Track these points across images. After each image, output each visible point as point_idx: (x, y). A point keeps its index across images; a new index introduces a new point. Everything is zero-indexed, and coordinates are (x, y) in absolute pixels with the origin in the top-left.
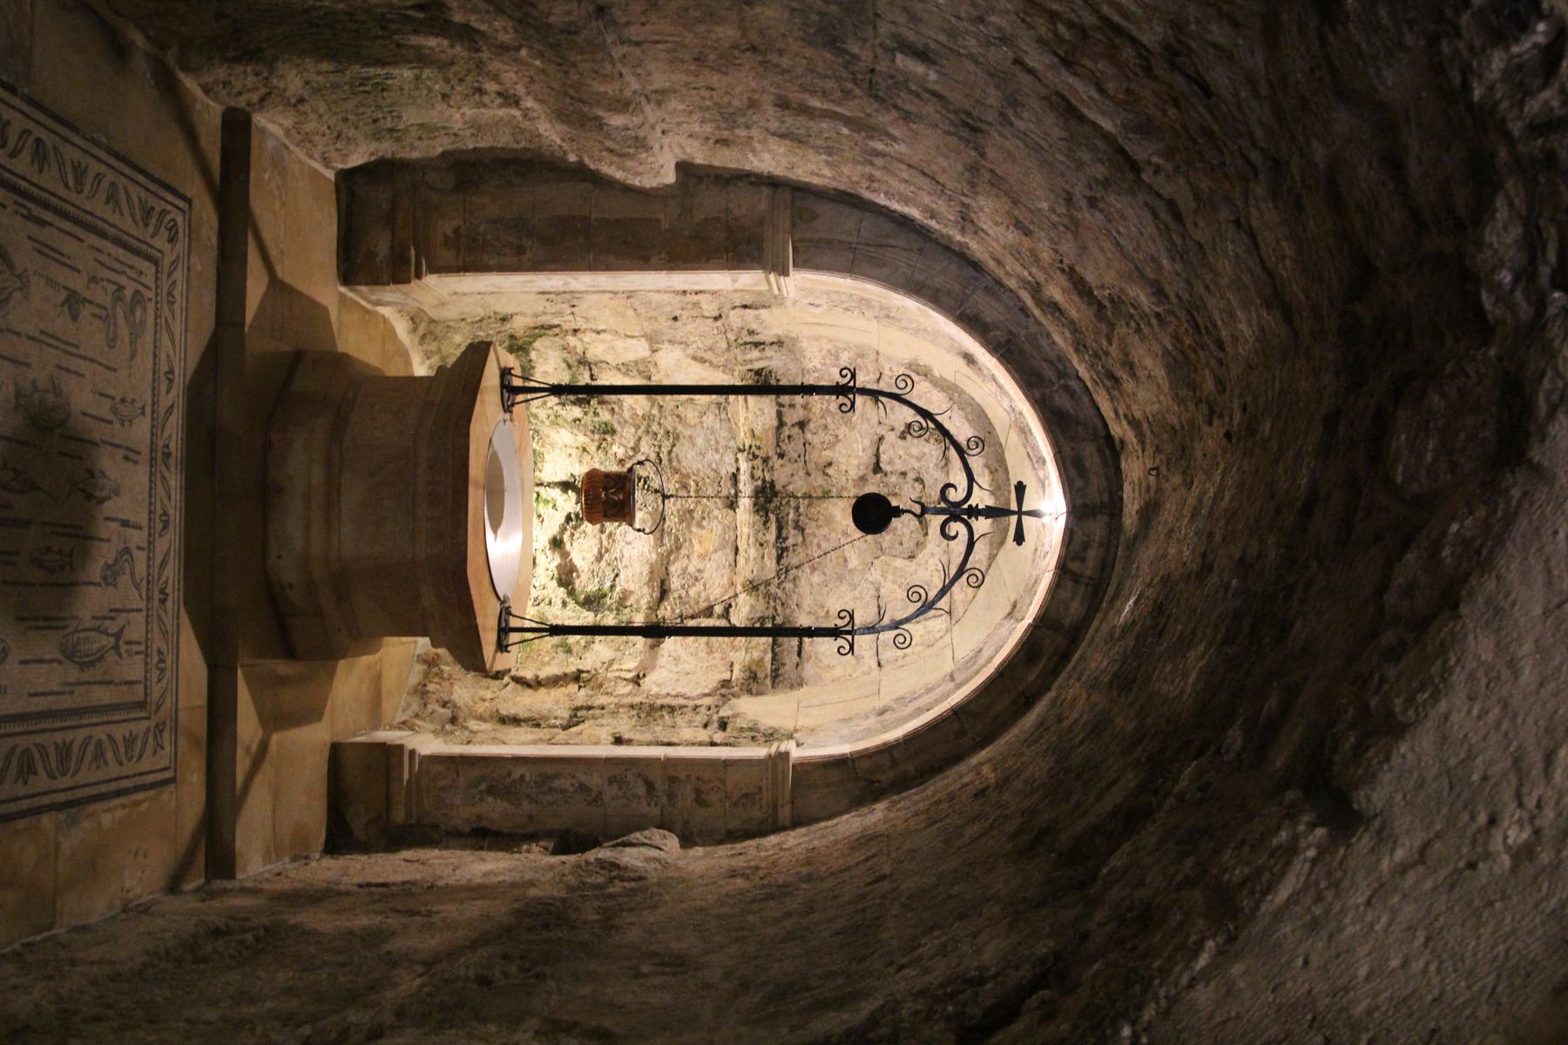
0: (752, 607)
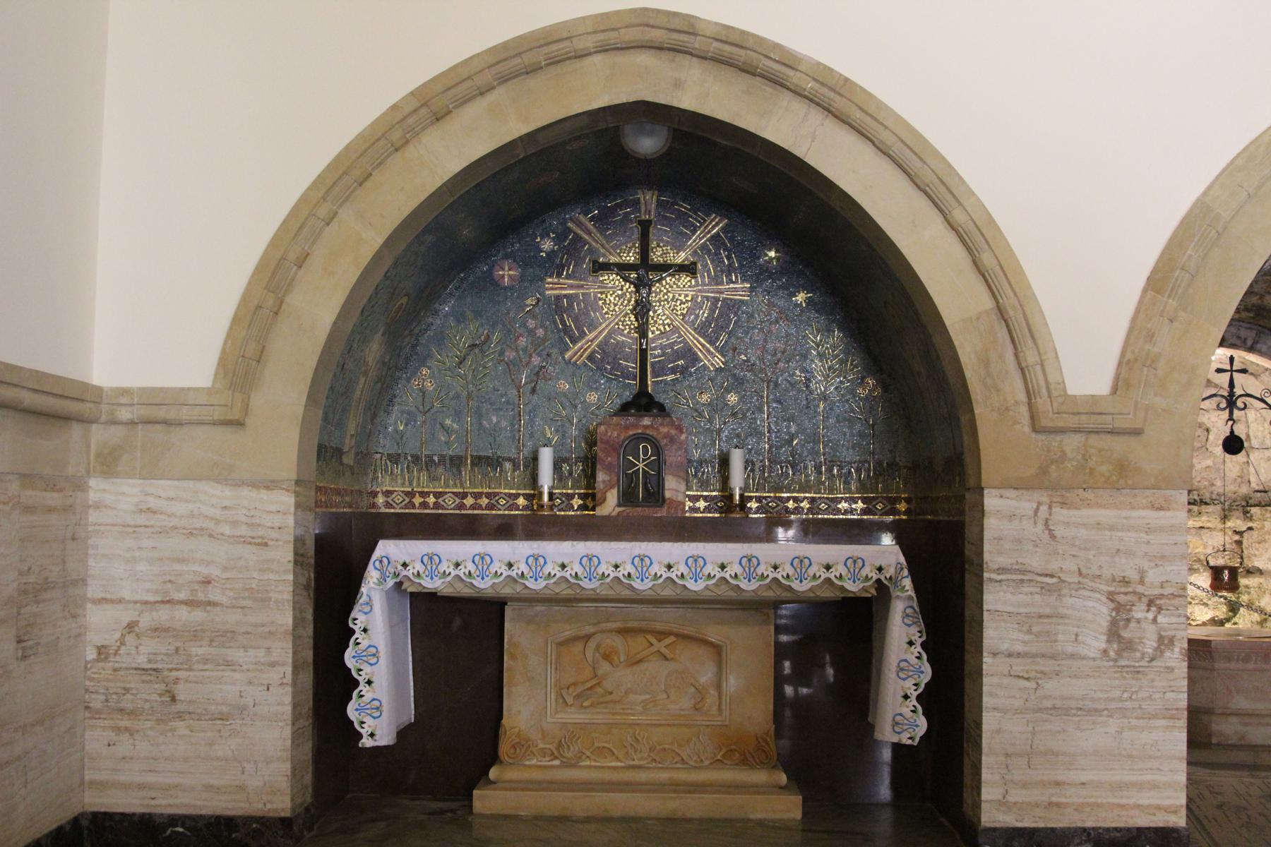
0: (1237, 518)
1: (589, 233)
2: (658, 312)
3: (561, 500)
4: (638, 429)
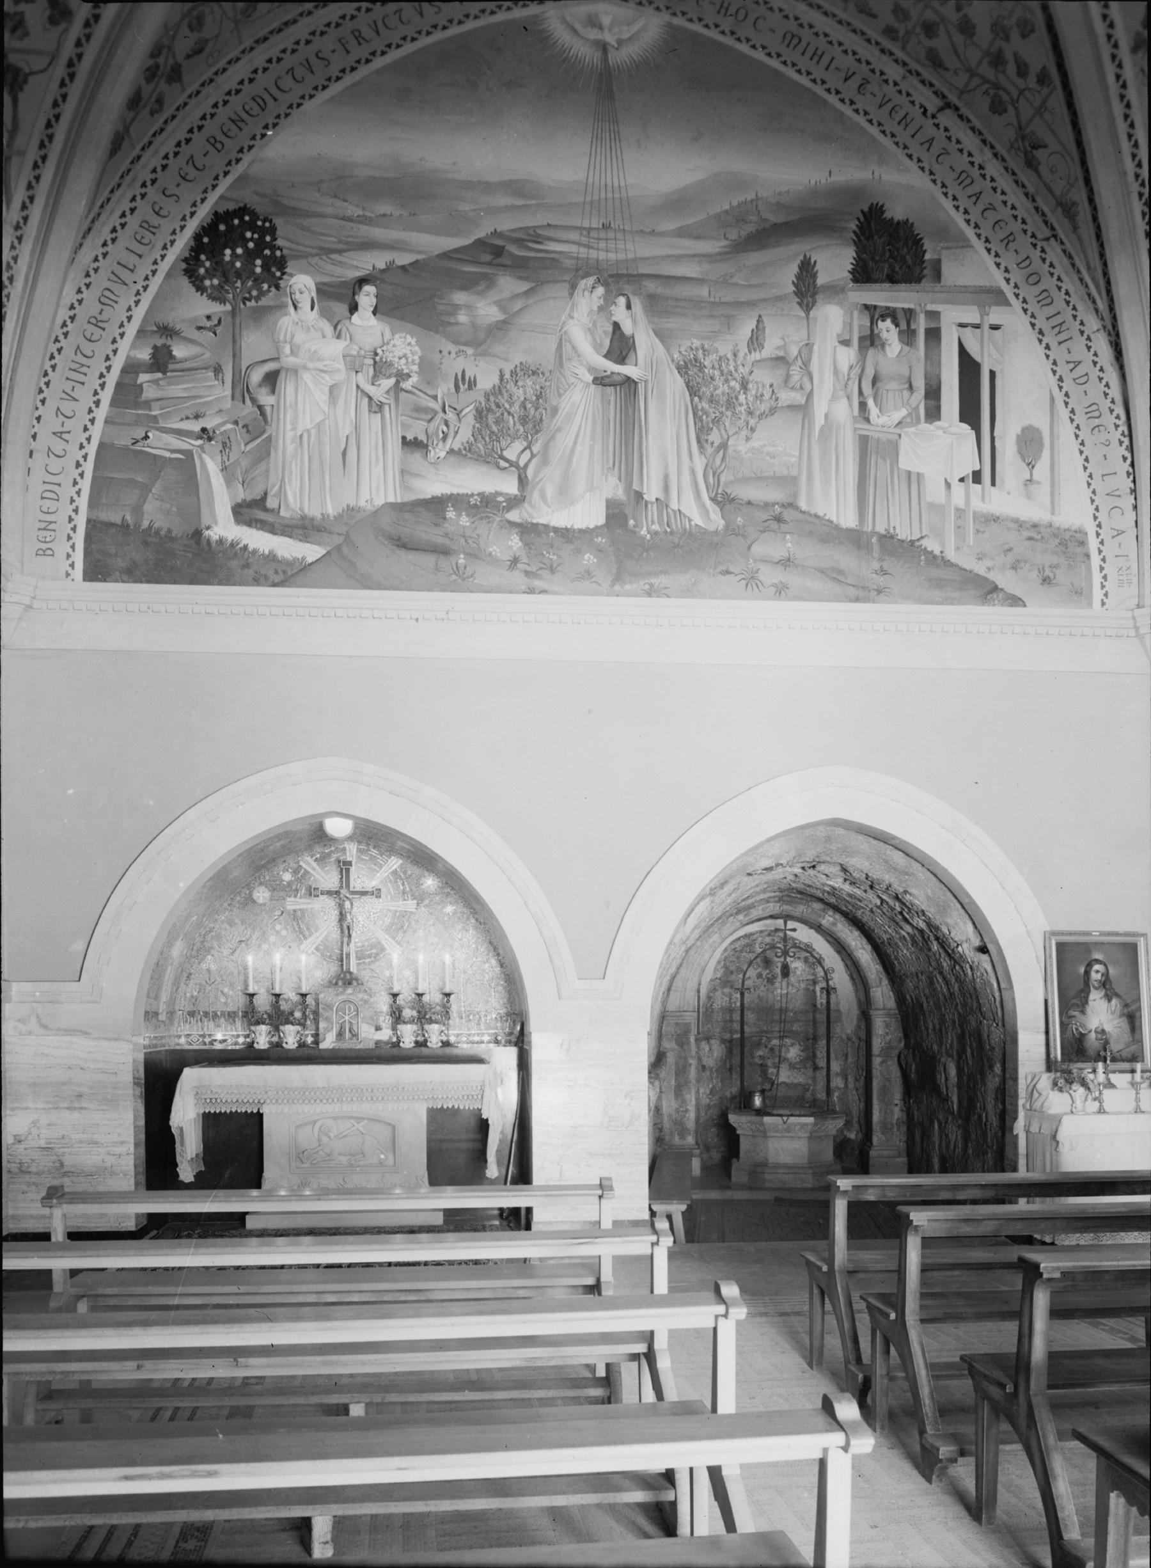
1: (314, 869)
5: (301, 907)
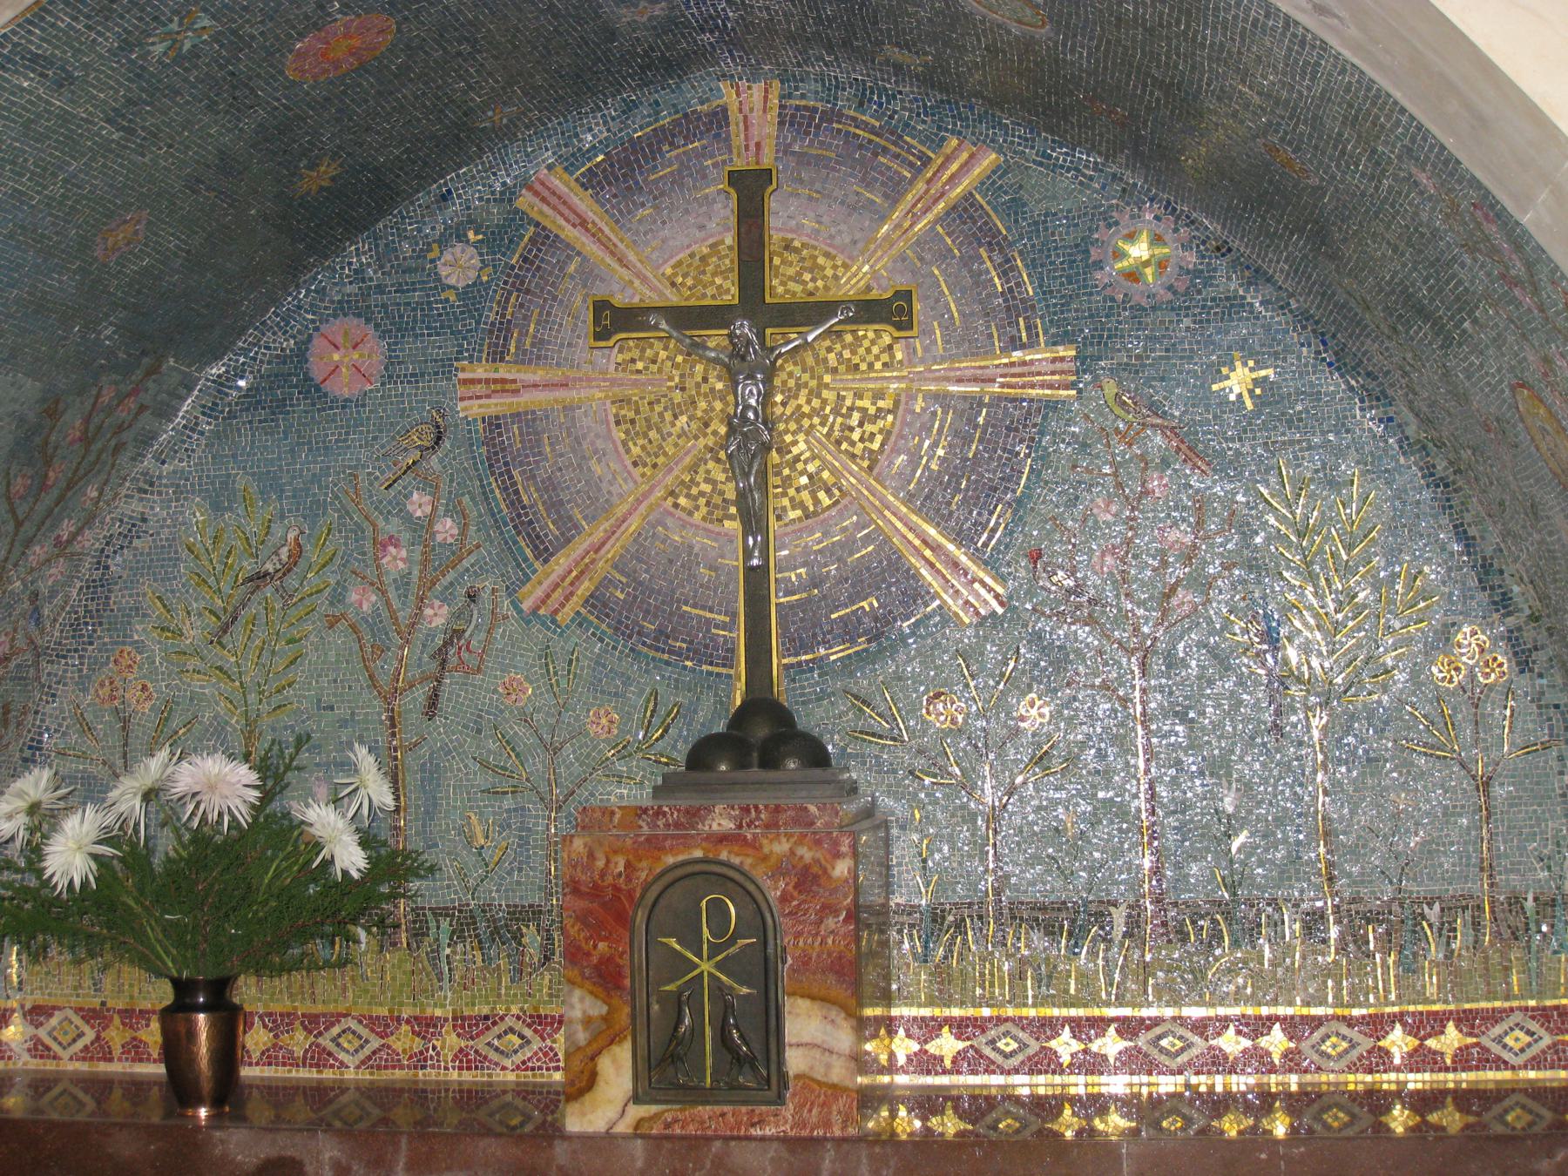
2: (795, 450)
3: (521, 1037)
4: (688, 847)
5: (526, 399)
